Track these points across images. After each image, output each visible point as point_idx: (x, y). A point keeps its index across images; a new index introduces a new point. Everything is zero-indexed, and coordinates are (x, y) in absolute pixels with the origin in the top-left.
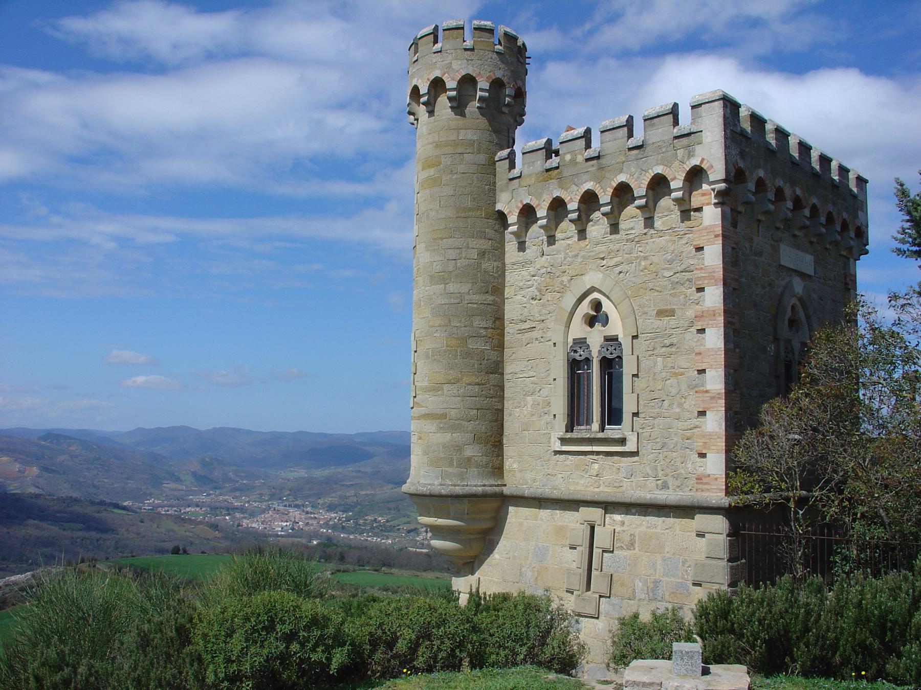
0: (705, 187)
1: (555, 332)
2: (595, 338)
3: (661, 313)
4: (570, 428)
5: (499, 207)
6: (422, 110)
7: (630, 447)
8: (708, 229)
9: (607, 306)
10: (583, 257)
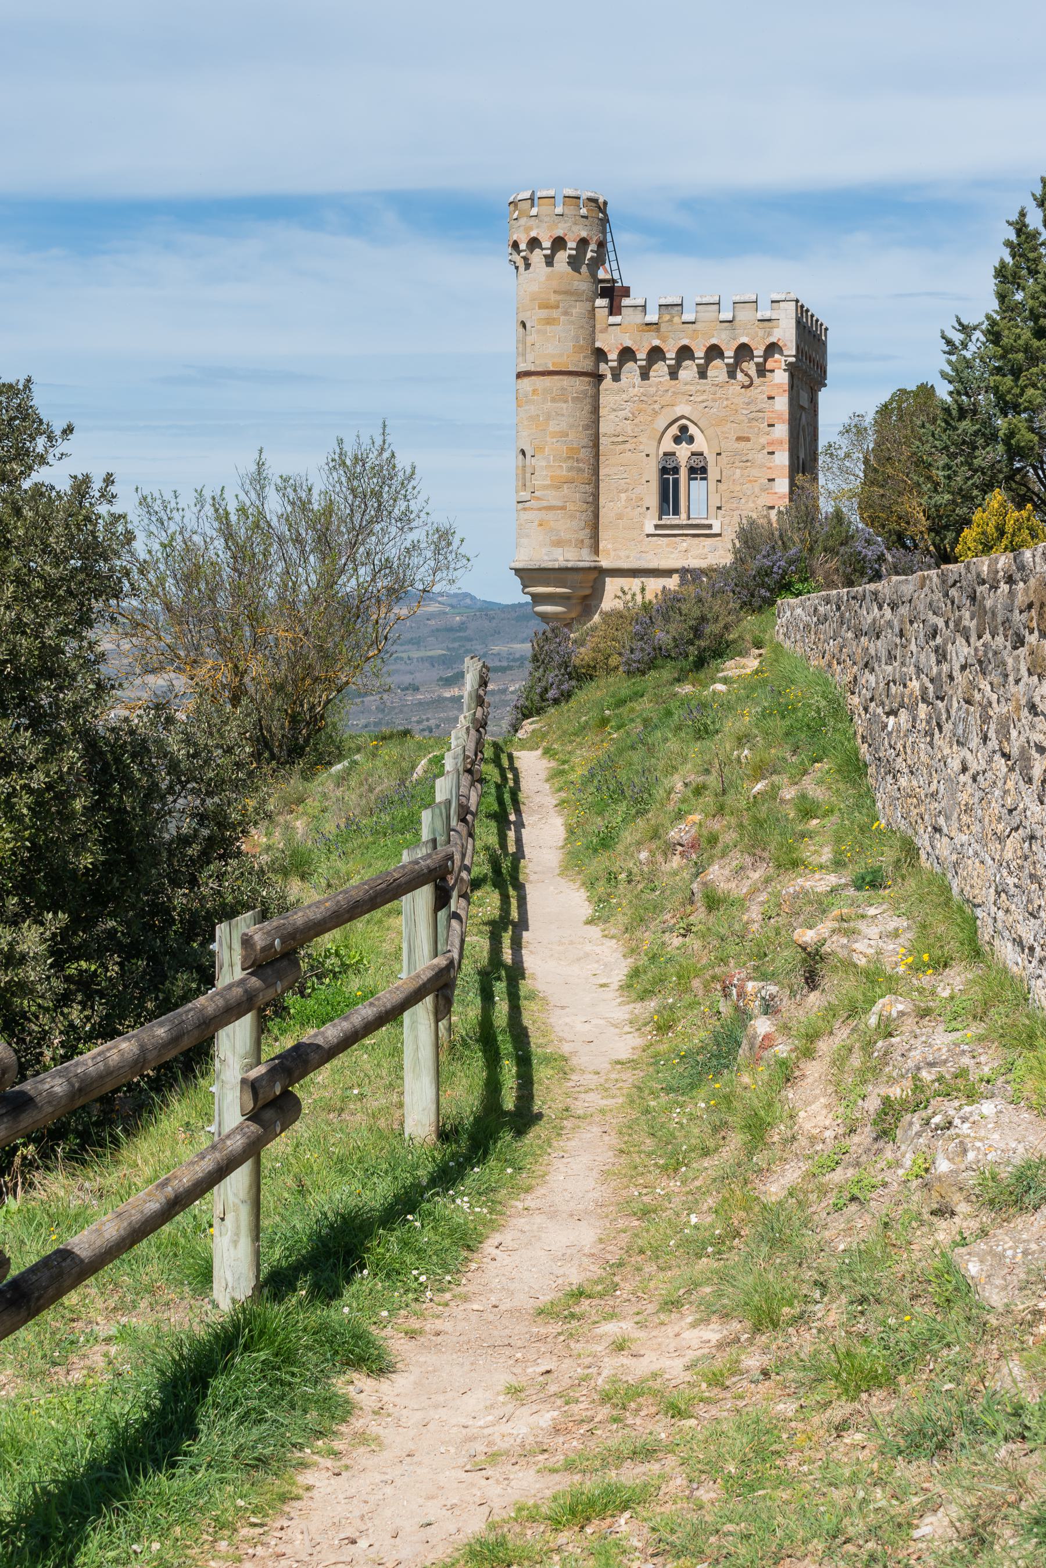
0: (777, 356)
1: (648, 445)
2: (683, 452)
3: (739, 439)
4: (660, 519)
5: (598, 345)
6: (537, 257)
7: (716, 530)
8: (779, 386)
9: (693, 430)
10: (674, 393)
